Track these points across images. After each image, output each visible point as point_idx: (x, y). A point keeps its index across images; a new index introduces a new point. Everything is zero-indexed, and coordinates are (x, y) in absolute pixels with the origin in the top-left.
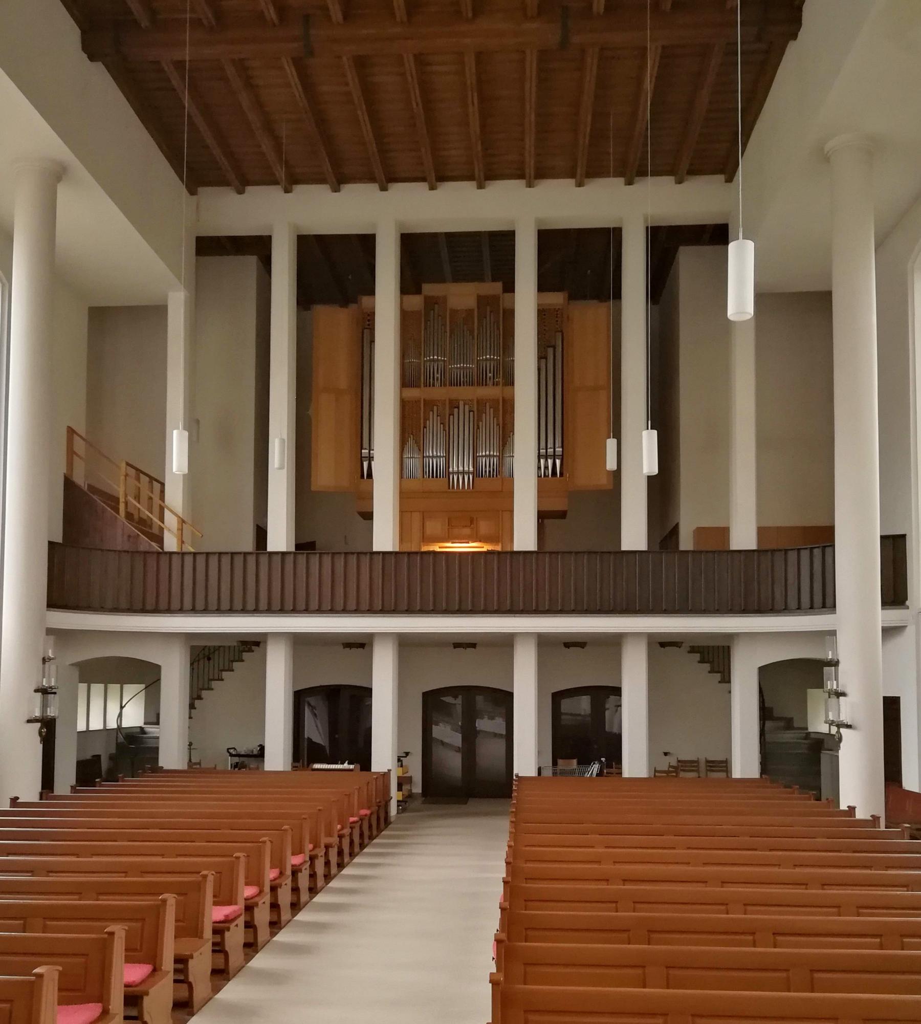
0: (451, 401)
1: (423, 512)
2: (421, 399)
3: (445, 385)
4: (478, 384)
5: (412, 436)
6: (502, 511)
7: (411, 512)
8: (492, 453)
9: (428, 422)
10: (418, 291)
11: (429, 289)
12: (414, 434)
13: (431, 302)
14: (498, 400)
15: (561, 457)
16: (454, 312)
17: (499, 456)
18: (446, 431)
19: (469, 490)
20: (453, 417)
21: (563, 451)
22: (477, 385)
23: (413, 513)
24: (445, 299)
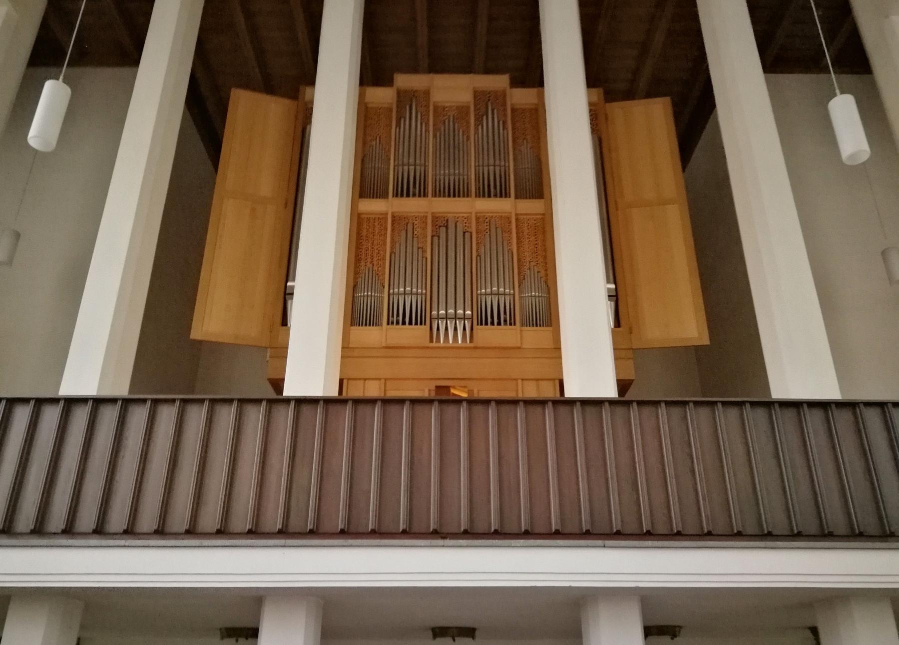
0: (435, 218)
1: (386, 380)
2: (387, 214)
3: (425, 195)
4: (478, 195)
5: (371, 265)
6: (522, 380)
7: (365, 379)
8: (502, 290)
9: (397, 245)
10: (389, 82)
11: (403, 81)
12: (375, 263)
13: (405, 98)
14: (509, 219)
15: (615, 298)
16: (440, 110)
17: (514, 294)
18: (426, 258)
19: (464, 345)
20: (439, 239)
21: (616, 288)
22: (476, 196)
23: (367, 381)
24: (427, 93)
